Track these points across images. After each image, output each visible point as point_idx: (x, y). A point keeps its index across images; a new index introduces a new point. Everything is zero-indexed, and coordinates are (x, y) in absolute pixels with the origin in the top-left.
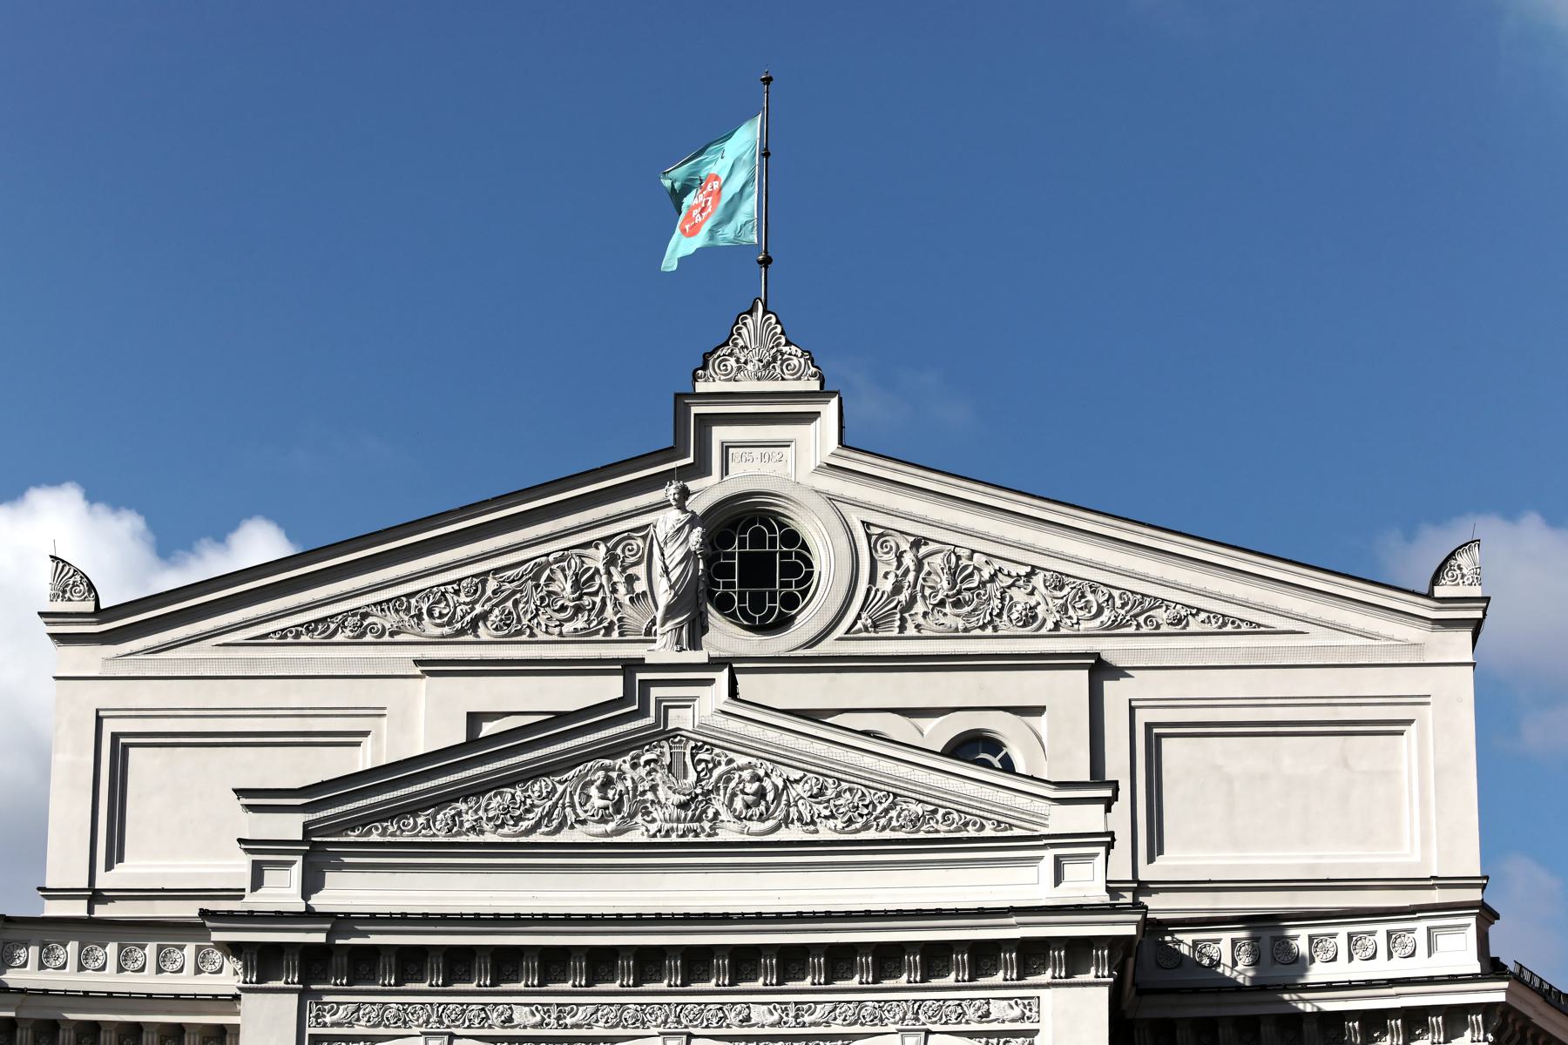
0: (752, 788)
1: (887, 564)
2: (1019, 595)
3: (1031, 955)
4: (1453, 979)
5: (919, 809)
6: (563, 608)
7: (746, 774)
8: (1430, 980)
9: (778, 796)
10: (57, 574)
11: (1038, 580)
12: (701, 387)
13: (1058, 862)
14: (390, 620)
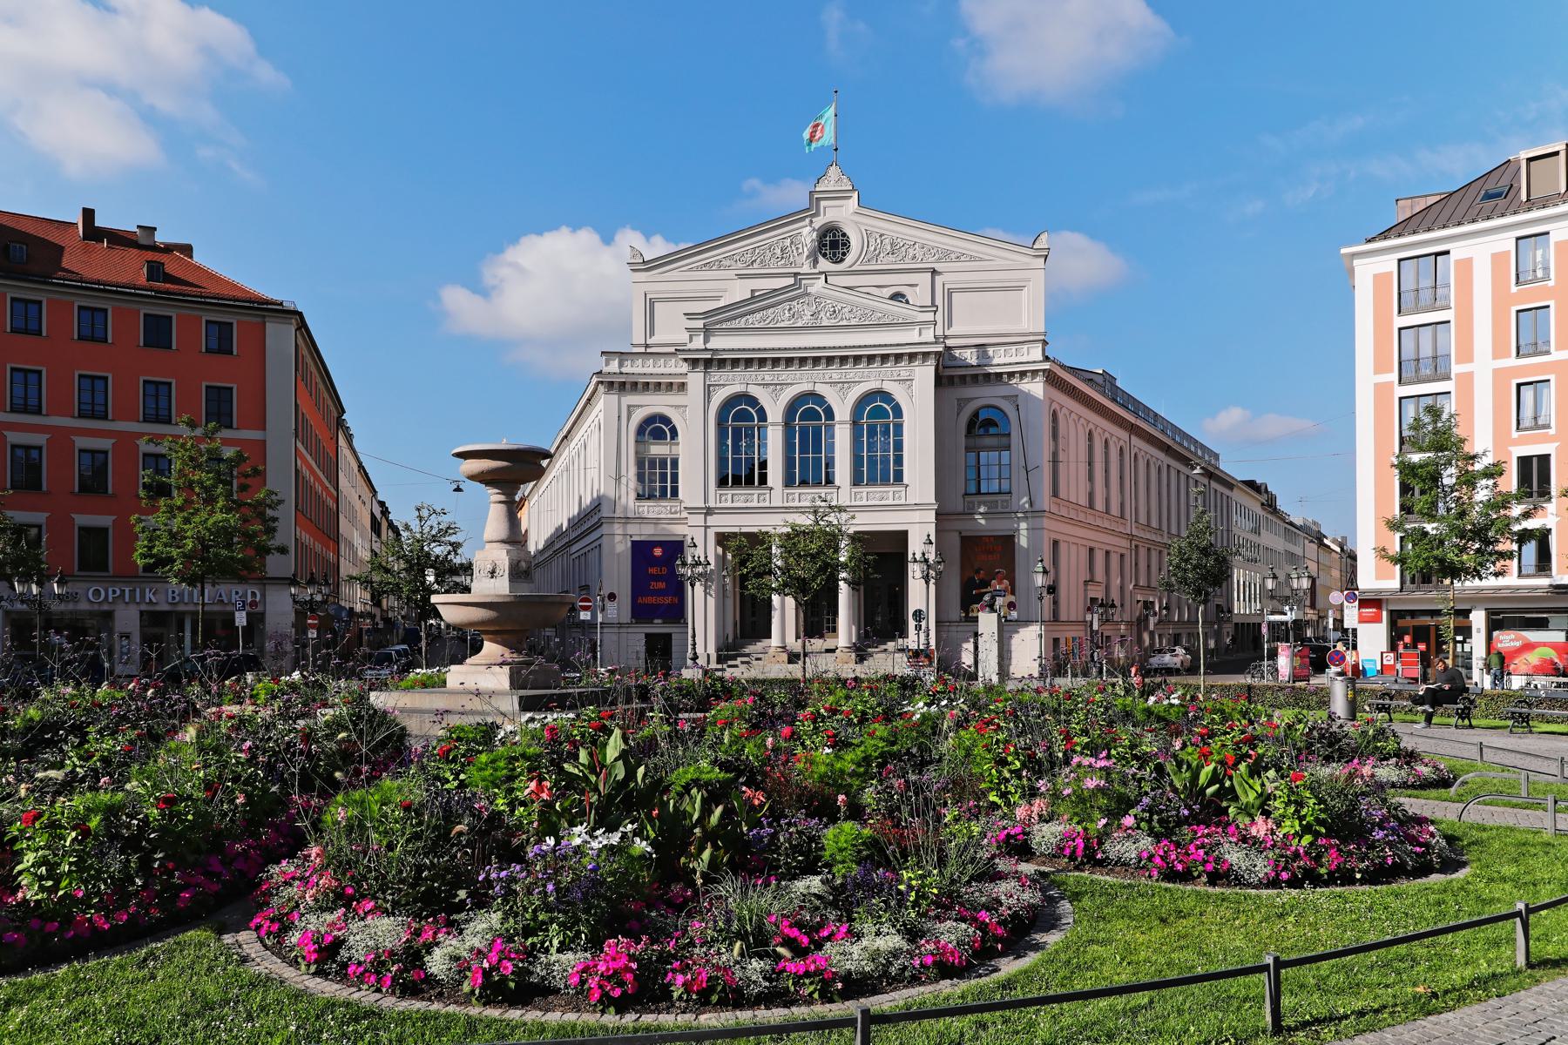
1: (872, 241)
14: (728, 263)
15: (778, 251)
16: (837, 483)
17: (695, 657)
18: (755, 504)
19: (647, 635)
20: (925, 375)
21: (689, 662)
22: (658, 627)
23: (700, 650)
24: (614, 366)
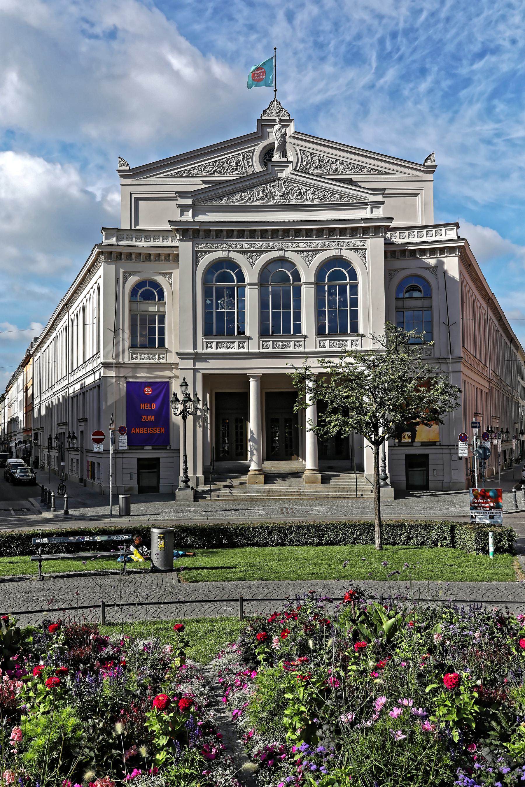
0: (298, 191)
2: (334, 165)
4: (452, 240)
5: (338, 196)
7: (297, 188)
8: (447, 241)
9: (304, 193)
10: (120, 161)
11: (338, 163)
12: (263, 118)
13: (372, 209)
14: (195, 171)
15: (233, 164)
16: (304, 332)
17: (187, 480)
18: (235, 350)
19: (139, 459)
20: (375, 246)
21: (182, 485)
22: (148, 452)
23: (190, 474)
24: (113, 241)
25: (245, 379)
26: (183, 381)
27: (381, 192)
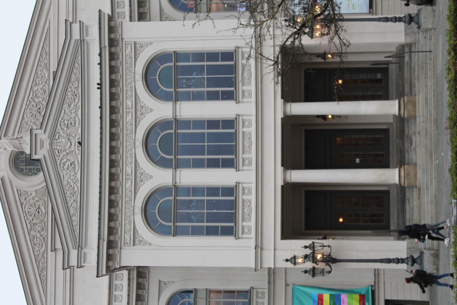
3: (112, 43)
6: (38, 212)
25: (289, 190)
26: (289, 263)
27: (68, 25)
